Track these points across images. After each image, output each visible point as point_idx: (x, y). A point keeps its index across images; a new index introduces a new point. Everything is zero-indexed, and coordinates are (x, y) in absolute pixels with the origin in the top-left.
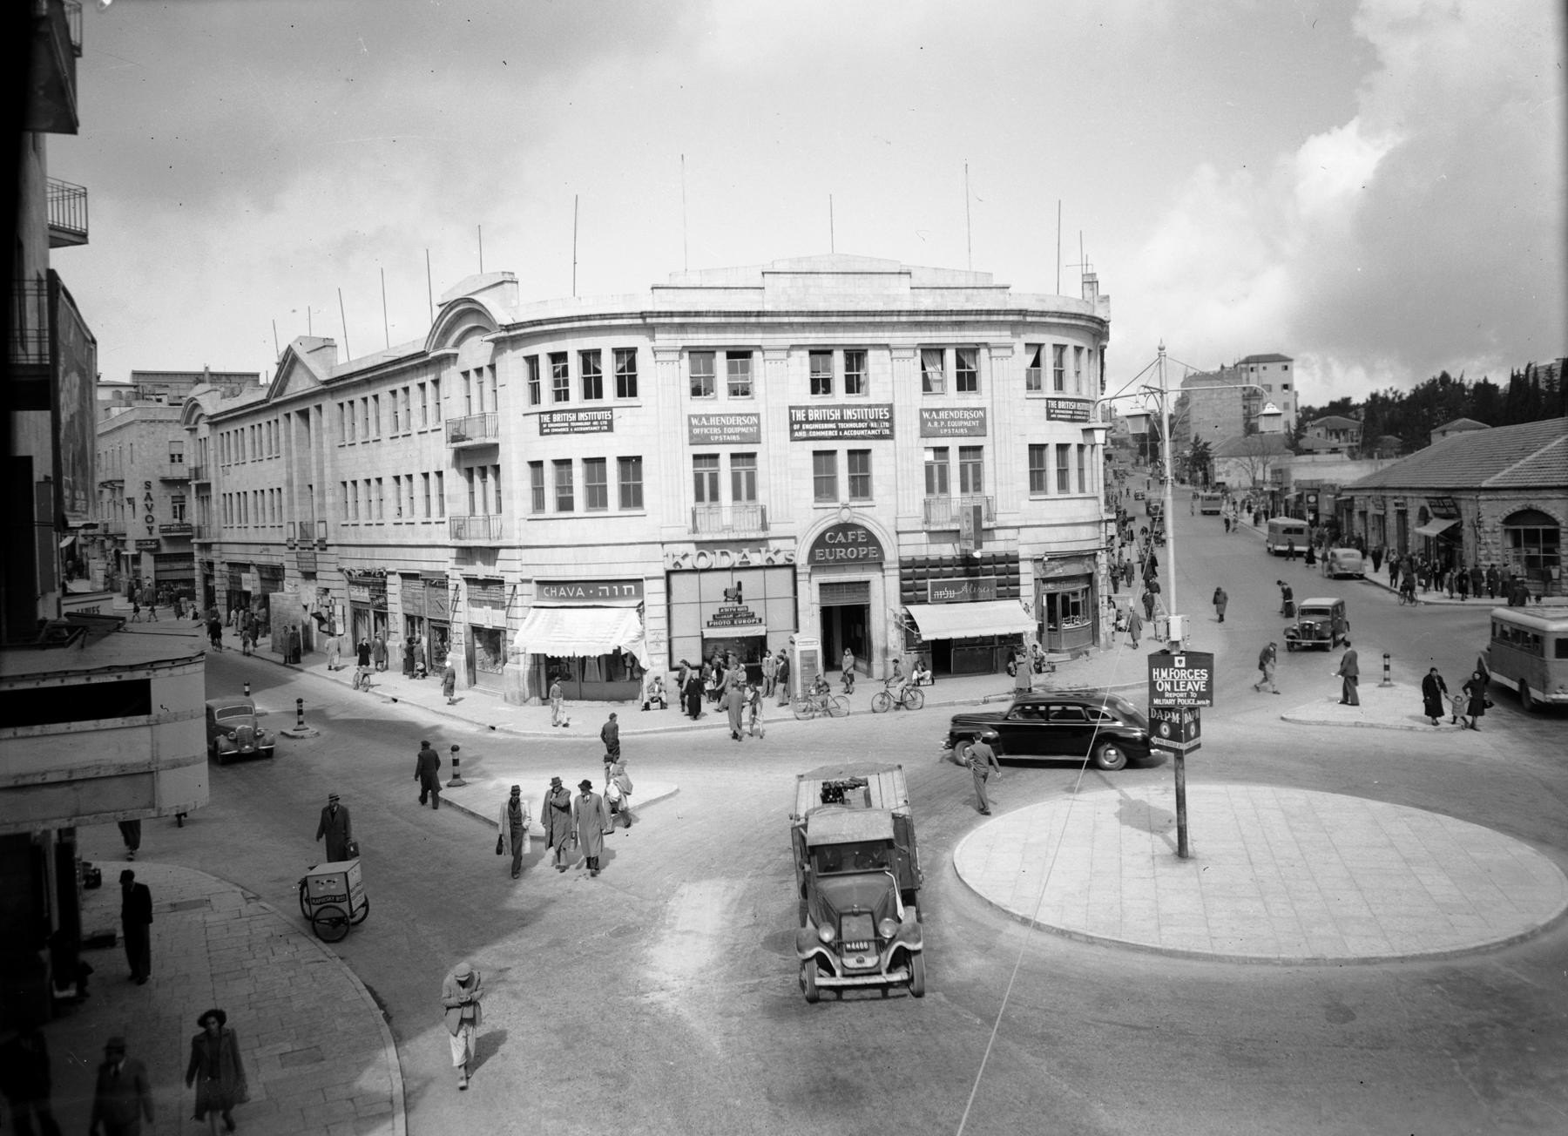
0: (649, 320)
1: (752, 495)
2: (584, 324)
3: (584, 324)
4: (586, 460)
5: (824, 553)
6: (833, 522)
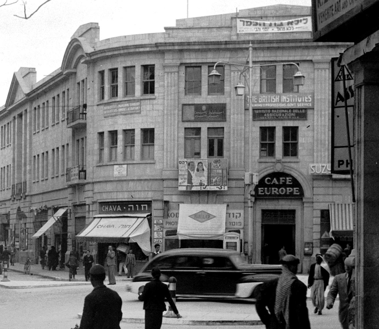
0: (160, 48)
1: (220, 153)
2: (126, 51)
3: (126, 51)
4: (125, 131)
5: (264, 190)
6: (271, 171)
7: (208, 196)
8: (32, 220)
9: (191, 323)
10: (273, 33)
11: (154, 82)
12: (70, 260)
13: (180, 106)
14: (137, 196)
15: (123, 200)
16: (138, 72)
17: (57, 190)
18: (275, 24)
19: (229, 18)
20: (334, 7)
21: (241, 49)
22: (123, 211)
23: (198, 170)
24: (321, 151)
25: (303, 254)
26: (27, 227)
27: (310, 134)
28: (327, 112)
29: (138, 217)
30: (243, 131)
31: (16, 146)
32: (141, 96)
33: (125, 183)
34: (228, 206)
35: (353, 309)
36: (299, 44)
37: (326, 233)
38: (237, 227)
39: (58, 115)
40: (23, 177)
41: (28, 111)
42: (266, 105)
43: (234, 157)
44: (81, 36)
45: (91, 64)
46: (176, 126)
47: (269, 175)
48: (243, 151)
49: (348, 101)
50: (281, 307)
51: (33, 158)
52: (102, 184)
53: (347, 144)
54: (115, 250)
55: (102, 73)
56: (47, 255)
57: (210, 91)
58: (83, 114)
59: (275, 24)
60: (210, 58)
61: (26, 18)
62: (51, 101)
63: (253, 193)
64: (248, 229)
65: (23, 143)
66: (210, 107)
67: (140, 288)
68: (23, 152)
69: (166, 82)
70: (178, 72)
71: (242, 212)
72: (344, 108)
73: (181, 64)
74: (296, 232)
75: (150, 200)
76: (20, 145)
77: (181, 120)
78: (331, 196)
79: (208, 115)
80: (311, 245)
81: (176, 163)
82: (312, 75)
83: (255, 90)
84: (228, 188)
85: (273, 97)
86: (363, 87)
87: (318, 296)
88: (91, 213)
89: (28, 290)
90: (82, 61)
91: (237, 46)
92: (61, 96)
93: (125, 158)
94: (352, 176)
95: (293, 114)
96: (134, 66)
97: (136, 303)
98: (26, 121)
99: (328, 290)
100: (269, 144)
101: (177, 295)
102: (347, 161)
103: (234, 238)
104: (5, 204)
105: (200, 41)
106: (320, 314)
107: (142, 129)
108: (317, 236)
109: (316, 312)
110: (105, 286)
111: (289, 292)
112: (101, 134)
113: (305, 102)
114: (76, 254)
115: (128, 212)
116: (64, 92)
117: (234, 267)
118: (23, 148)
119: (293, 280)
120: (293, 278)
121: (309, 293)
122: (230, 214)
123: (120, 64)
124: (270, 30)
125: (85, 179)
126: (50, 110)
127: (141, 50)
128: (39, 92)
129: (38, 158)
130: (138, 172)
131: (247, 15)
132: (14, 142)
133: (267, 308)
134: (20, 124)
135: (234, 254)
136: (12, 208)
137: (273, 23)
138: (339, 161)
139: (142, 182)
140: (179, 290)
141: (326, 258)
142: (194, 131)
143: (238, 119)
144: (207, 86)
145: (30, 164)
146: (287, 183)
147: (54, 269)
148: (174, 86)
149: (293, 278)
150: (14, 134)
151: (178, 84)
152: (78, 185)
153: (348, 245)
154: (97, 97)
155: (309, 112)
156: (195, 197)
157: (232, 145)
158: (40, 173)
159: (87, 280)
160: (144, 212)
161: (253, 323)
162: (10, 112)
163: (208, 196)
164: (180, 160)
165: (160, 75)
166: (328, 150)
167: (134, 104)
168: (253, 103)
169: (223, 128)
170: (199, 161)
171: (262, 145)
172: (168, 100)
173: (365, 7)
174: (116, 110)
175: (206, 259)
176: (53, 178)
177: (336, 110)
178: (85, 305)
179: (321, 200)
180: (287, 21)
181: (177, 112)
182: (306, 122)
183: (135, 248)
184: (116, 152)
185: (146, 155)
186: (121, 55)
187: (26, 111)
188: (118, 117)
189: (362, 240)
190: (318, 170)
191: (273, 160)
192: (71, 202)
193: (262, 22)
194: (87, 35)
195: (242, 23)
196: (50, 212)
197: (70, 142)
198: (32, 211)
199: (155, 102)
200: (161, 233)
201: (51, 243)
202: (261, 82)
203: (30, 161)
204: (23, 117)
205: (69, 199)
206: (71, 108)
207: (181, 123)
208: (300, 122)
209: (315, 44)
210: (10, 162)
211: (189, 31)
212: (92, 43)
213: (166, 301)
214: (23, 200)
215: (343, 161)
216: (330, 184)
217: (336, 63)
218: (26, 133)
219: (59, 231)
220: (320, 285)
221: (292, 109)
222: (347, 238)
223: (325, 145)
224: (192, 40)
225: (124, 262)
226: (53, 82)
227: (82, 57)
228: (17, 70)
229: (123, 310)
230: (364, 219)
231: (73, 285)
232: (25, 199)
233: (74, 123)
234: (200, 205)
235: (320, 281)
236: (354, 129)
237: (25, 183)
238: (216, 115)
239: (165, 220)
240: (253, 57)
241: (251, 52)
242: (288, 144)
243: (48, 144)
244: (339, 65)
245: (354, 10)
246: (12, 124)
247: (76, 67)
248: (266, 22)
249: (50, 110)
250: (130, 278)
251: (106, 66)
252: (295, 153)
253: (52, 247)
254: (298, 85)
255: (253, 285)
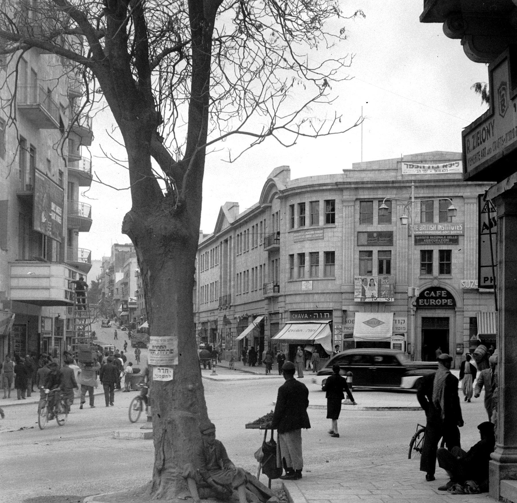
0: (339, 186)
1: (388, 272)
2: (312, 189)
3: (312, 189)
4: (311, 253)
5: (424, 302)
6: (429, 286)
7: (378, 306)
8: (235, 326)
9: (364, 409)
10: (431, 174)
11: (334, 214)
12: (266, 358)
13: (356, 233)
14: (321, 306)
15: (310, 309)
16: (322, 206)
17: (256, 302)
18: (433, 167)
19: (395, 162)
20: (480, 153)
21: (405, 187)
22: (309, 318)
23: (370, 285)
24: (470, 270)
25: (455, 353)
26: (232, 331)
27: (461, 256)
28: (475, 238)
29: (322, 323)
30: (407, 254)
31: (223, 266)
32: (325, 225)
33: (311, 295)
34: (394, 314)
35: (496, 397)
36: (452, 183)
37: (474, 336)
38: (402, 331)
39: (257, 241)
40: (228, 291)
41: (232, 237)
42: (426, 232)
43: (399, 274)
44: (275, 176)
45: (284, 200)
46: (353, 250)
47: (427, 289)
48: (407, 269)
49: (492, 229)
50: (437, 396)
51: (236, 276)
52: (292, 296)
53: (491, 264)
54: (303, 350)
55: (292, 206)
56: (247, 354)
57: (380, 221)
58: (277, 239)
59: (433, 167)
60: (380, 194)
61: (231, 162)
62: (251, 229)
63: (415, 304)
64: (411, 333)
65: (228, 263)
66: (380, 234)
67: (323, 381)
68: (228, 271)
69: (344, 214)
70: (354, 206)
71: (406, 319)
72: (489, 235)
73: (357, 199)
74: (450, 336)
75: (331, 309)
76: (226, 265)
77: (356, 244)
78: (478, 306)
79: (378, 240)
80: (462, 346)
81: (352, 279)
82: (462, 208)
83: (416, 220)
84: (395, 299)
85: (431, 226)
86: (504, 218)
87: (467, 387)
88: (283, 320)
89: (233, 382)
90: (276, 197)
91: (402, 185)
92: (259, 225)
93: (311, 275)
94: (495, 290)
95: (447, 240)
96: (319, 201)
97: (320, 393)
98: (230, 245)
99: (475, 382)
100: (428, 264)
101: (353, 387)
102: (491, 278)
103: (399, 340)
104: (214, 313)
105: (372, 180)
106: (469, 401)
107: (324, 252)
108: (466, 339)
109: (466, 400)
110: (295, 379)
111: (444, 383)
112: (292, 256)
113: (457, 230)
114: (271, 353)
115: (313, 319)
116: (261, 222)
117: (399, 364)
118: (228, 267)
119: (448, 374)
120: (447, 373)
121: (460, 385)
122: (396, 321)
123: (307, 200)
124: (429, 172)
125: (279, 292)
126: (251, 236)
127: (324, 188)
128: (241, 222)
129: (241, 276)
130: (321, 287)
131: (410, 159)
132: (221, 263)
133: (426, 397)
134: (226, 248)
135: (400, 353)
136: (219, 316)
137: (431, 166)
138: (485, 278)
139: (325, 295)
140: (355, 382)
141: (474, 357)
142: (367, 254)
143: (402, 244)
144: (377, 217)
145: (234, 280)
146: (443, 296)
147: (254, 365)
148: (351, 217)
149: (447, 373)
150: (221, 256)
151: (354, 216)
152: (273, 297)
153: (492, 346)
154: (288, 226)
155: (460, 238)
156: (368, 307)
157: (398, 265)
158: (242, 288)
159: (280, 374)
160: (327, 319)
161: (415, 409)
162: (218, 238)
163: (378, 306)
164: (355, 277)
165: (340, 208)
166: (476, 269)
167: (318, 232)
168: (415, 231)
169: (391, 251)
170: (371, 278)
171: (422, 265)
172: (346, 228)
173: (505, 153)
174: (303, 237)
175: (377, 357)
176: (252, 291)
177: (482, 236)
178: (279, 394)
179: (470, 310)
180: (442, 165)
181: (353, 238)
182: (458, 246)
183: (319, 348)
184: (304, 271)
185: (328, 273)
186: (308, 192)
187: (231, 237)
188: (305, 242)
189: (503, 342)
190: (468, 285)
191: (431, 277)
192: (267, 311)
193: (422, 165)
194: (280, 176)
195: (406, 166)
196: (250, 319)
197: (267, 263)
198: (235, 318)
199: (335, 230)
200: (340, 336)
201: (251, 344)
202: (421, 214)
203: (234, 278)
204: (229, 242)
205: (265, 308)
206: (267, 235)
207: (356, 247)
208: (453, 246)
209: (465, 183)
210: (218, 279)
211: (363, 172)
212: (285, 182)
213: (344, 391)
214: (228, 310)
215: (488, 278)
216: (477, 296)
217: (482, 198)
218: (230, 255)
219: (257, 334)
220: (470, 379)
221: (446, 236)
222: (491, 340)
223: (473, 265)
224: (365, 180)
225: (310, 359)
226: (253, 214)
227: (276, 193)
228: (223, 204)
229: (309, 398)
230: (505, 325)
231: (269, 378)
232: (230, 308)
233: (270, 247)
234: (372, 314)
235: (469, 375)
236: (497, 252)
237: (230, 295)
238: (384, 240)
239: (344, 326)
240: (415, 194)
241: (413, 189)
242: (443, 264)
243: (249, 264)
244: (484, 200)
245: (497, 156)
246: (219, 247)
247: (271, 202)
248: (425, 165)
249: (251, 236)
250: (315, 373)
251: (296, 201)
252: (449, 272)
253: (252, 347)
254: (451, 217)
255: (415, 378)
